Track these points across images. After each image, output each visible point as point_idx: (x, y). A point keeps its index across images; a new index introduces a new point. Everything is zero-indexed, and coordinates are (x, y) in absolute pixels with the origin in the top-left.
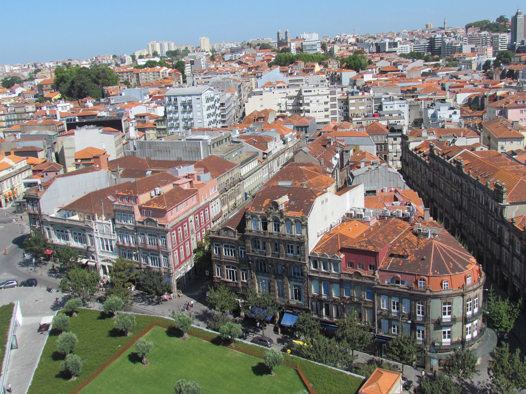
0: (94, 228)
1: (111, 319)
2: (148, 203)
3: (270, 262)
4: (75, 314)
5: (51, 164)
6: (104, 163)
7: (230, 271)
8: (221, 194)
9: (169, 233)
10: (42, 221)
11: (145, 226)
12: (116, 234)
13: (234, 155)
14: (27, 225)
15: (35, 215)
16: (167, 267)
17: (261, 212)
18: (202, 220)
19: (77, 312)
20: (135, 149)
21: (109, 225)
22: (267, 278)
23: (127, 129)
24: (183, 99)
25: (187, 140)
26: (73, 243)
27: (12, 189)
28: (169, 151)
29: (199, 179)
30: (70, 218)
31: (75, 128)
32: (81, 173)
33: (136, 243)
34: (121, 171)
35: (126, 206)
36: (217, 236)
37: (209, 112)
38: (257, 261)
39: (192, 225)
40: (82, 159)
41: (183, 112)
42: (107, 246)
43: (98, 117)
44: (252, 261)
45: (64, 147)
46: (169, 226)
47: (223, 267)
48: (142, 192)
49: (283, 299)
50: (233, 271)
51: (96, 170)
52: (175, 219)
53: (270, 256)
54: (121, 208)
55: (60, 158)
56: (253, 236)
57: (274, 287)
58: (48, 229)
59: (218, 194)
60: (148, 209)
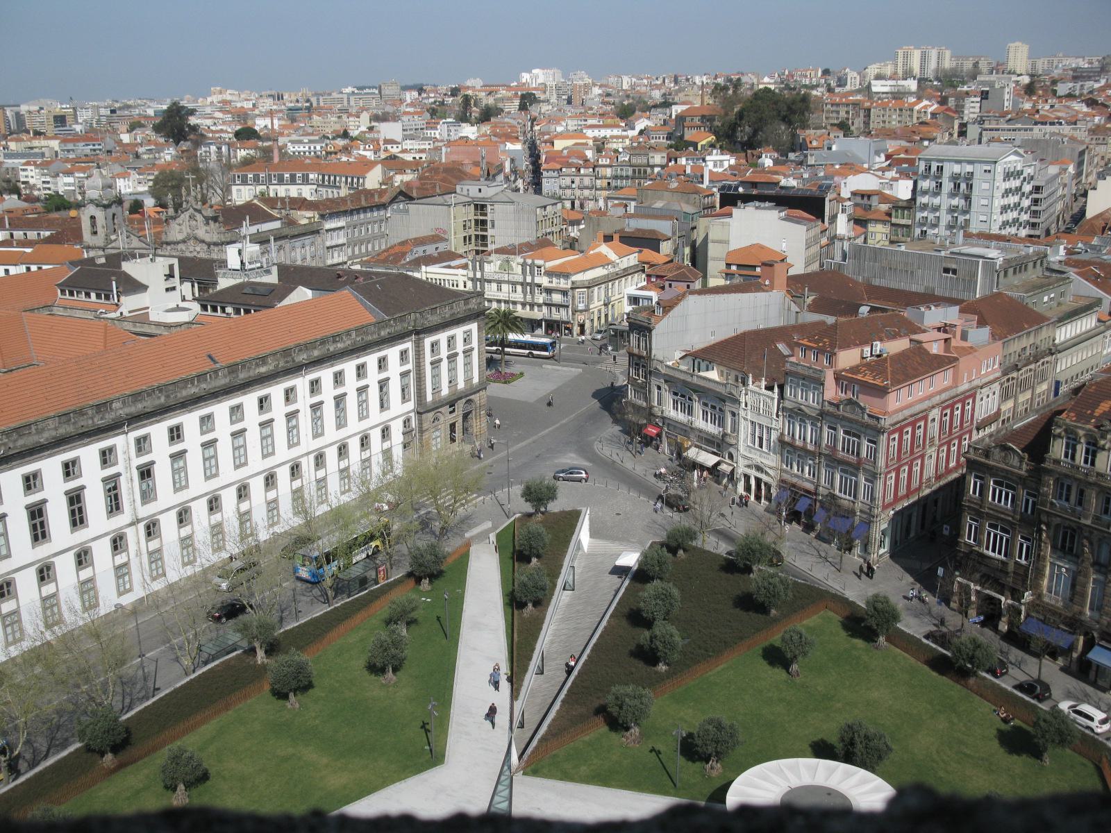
0: (742, 399)
2: (855, 370)
3: (1086, 534)
4: (681, 552)
5: (680, 268)
6: (781, 280)
7: (995, 536)
8: (1005, 373)
9: (886, 435)
10: (650, 372)
11: (841, 412)
12: (781, 418)
13: (1046, 299)
14: (622, 373)
15: (640, 357)
16: (869, 502)
17: (1088, 427)
18: (957, 422)
19: (685, 550)
20: (844, 259)
21: (773, 399)
22: (1074, 567)
23: (833, 218)
24: (957, 168)
25: (952, 253)
26: (701, 422)
27: (606, 305)
28: (912, 272)
29: (964, 337)
30: (702, 374)
31: (735, 205)
32: (735, 292)
33: (818, 444)
34: (811, 298)
35: (810, 368)
36: (983, 460)
37: (1006, 201)
38: (1058, 526)
39: (934, 429)
40: (739, 266)
41: (952, 195)
42: (761, 439)
43: (782, 188)
44: (1047, 525)
45: (710, 237)
46: (886, 422)
47: (982, 525)
48: (847, 345)
49: (1096, 615)
50: (1001, 538)
51: (764, 291)
52: (901, 409)
53: (1088, 522)
54: (799, 369)
55: (698, 257)
56: (1060, 474)
57: (1084, 586)
58: (659, 388)
59: (998, 374)
60: (851, 381)
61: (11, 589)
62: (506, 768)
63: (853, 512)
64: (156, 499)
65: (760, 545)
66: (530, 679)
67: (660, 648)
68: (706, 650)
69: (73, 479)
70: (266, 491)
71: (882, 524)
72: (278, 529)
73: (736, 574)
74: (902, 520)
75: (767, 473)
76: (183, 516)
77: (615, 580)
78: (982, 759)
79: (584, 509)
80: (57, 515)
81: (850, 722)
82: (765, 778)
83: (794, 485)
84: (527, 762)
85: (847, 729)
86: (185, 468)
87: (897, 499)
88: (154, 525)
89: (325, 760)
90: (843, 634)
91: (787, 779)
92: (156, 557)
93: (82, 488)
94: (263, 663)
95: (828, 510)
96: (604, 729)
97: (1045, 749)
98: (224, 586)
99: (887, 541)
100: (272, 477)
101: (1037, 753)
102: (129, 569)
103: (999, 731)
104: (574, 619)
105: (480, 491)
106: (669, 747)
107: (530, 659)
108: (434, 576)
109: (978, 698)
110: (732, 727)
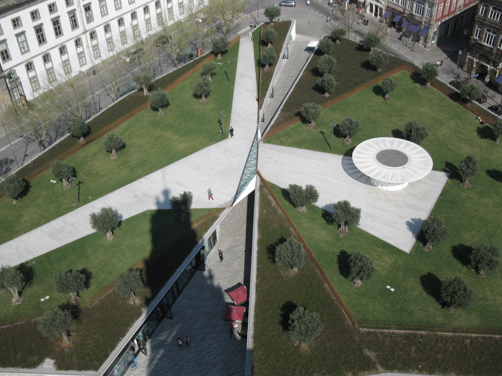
1: (367, 53)
4: (338, 41)
19: (340, 40)
61: (32, 66)
62: (255, 140)
63: (421, 23)
64: (93, 20)
65: (375, 38)
66: (267, 100)
67: (326, 86)
68: (347, 87)
69: (54, 13)
70: (145, 15)
71: (434, 29)
72: (151, 33)
73: (363, 52)
74: (444, 27)
75: (381, 3)
76: (107, 28)
77: (307, 54)
78: (469, 140)
79: (293, 20)
80: (49, 30)
81: (410, 122)
82: (370, 146)
83: (393, 9)
84: (265, 137)
85: (409, 125)
86: (106, 5)
87: (443, 16)
88: (94, 33)
89: (176, 138)
90: (411, 81)
91: (380, 146)
92: (96, 48)
93: (59, 17)
94: (147, 95)
95: (409, 21)
96: (300, 122)
97: (498, 136)
98: (128, 60)
99: (436, 37)
100: (147, 8)
101: (494, 138)
102: (84, 54)
103: (478, 128)
104: (287, 72)
105: (244, 12)
106: (328, 131)
107: (267, 91)
108: (223, 53)
109: (471, 113)
110: (357, 122)
